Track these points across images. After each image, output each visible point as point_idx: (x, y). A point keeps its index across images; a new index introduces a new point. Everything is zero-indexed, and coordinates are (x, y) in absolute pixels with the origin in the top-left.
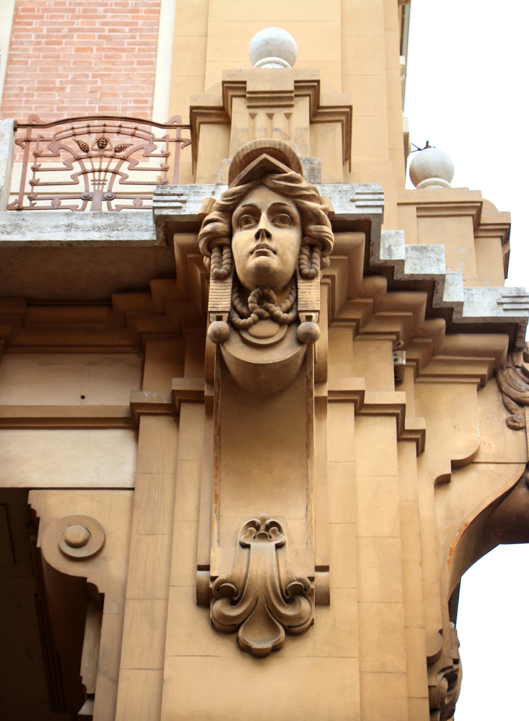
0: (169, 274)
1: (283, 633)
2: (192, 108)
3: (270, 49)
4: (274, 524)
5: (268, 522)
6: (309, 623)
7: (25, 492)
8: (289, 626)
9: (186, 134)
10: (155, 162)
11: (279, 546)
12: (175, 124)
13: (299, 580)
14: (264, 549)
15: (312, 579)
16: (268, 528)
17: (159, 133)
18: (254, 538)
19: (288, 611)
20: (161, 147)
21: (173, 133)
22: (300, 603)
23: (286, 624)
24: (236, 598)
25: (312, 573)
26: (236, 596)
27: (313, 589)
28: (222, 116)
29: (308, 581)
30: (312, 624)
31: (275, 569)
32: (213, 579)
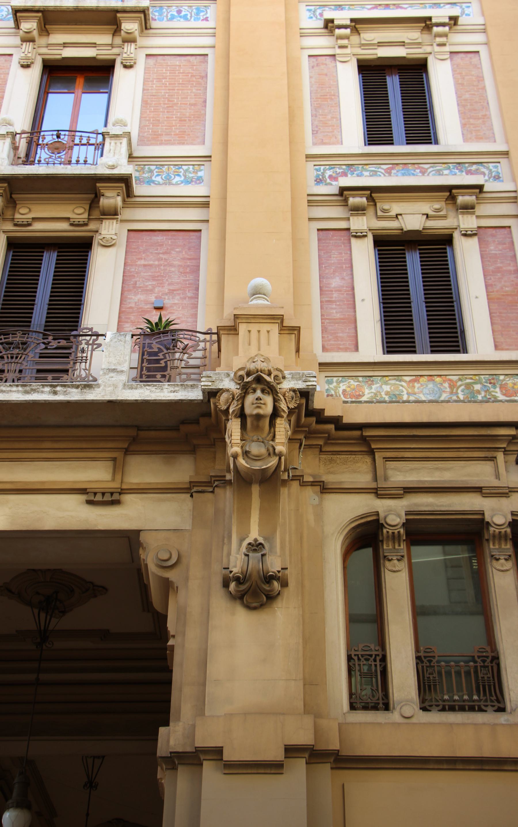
0: (208, 414)
2: (218, 327)
3: (257, 292)
6: (278, 592)
7: (138, 532)
9: (215, 337)
10: (199, 354)
12: (209, 332)
13: (272, 572)
14: (255, 556)
15: (279, 572)
16: (257, 546)
17: (202, 337)
19: (266, 587)
20: (202, 345)
21: (208, 337)
22: (273, 584)
23: (266, 593)
25: (280, 569)
27: (279, 577)
28: (233, 330)
30: (279, 594)
31: (261, 568)
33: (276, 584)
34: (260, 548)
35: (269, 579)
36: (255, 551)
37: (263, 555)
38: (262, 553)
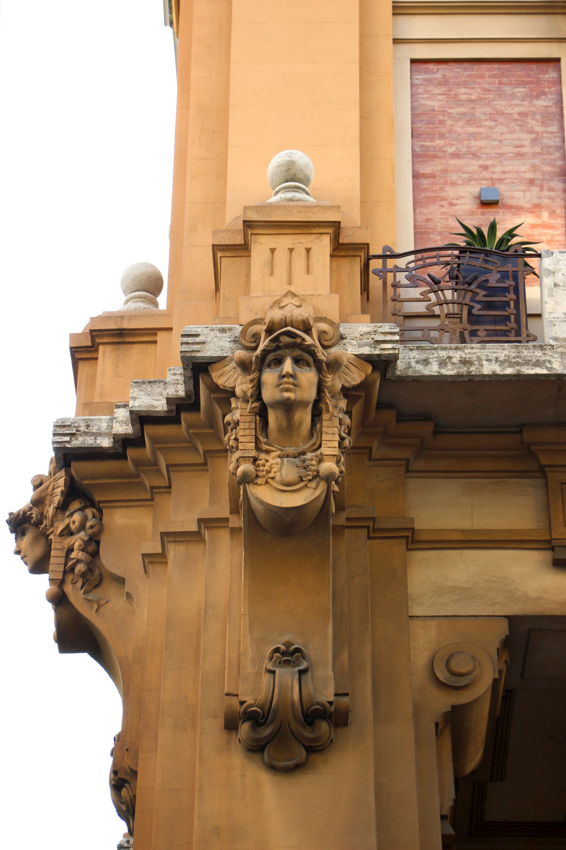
1: (304, 752)
4: (298, 650)
5: (292, 648)
6: (329, 742)
8: (310, 746)
11: (302, 673)
13: (318, 704)
15: (331, 703)
18: (280, 663)
19: (307, 733)
23: (307, 744)
24: (262, 721)
25: (332, 698)
26: (262, 719)
27: (332, 712)
29: (328, 704)
32: (242, 703)
33: (324, 727)
34: (297, 658)
35: (313, 715)
36: (287, 662)
37: (302, 673)
38: (301, 668)
